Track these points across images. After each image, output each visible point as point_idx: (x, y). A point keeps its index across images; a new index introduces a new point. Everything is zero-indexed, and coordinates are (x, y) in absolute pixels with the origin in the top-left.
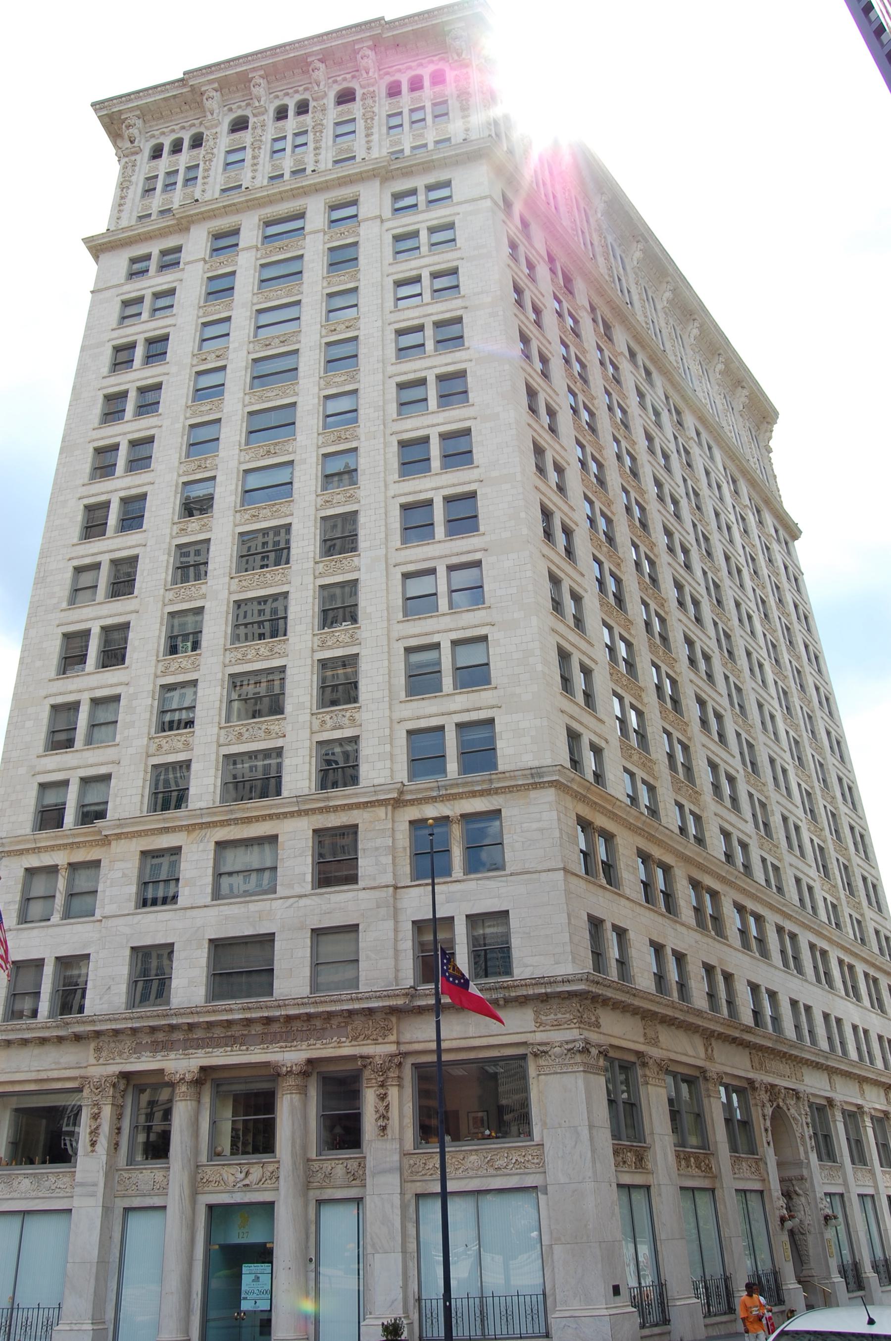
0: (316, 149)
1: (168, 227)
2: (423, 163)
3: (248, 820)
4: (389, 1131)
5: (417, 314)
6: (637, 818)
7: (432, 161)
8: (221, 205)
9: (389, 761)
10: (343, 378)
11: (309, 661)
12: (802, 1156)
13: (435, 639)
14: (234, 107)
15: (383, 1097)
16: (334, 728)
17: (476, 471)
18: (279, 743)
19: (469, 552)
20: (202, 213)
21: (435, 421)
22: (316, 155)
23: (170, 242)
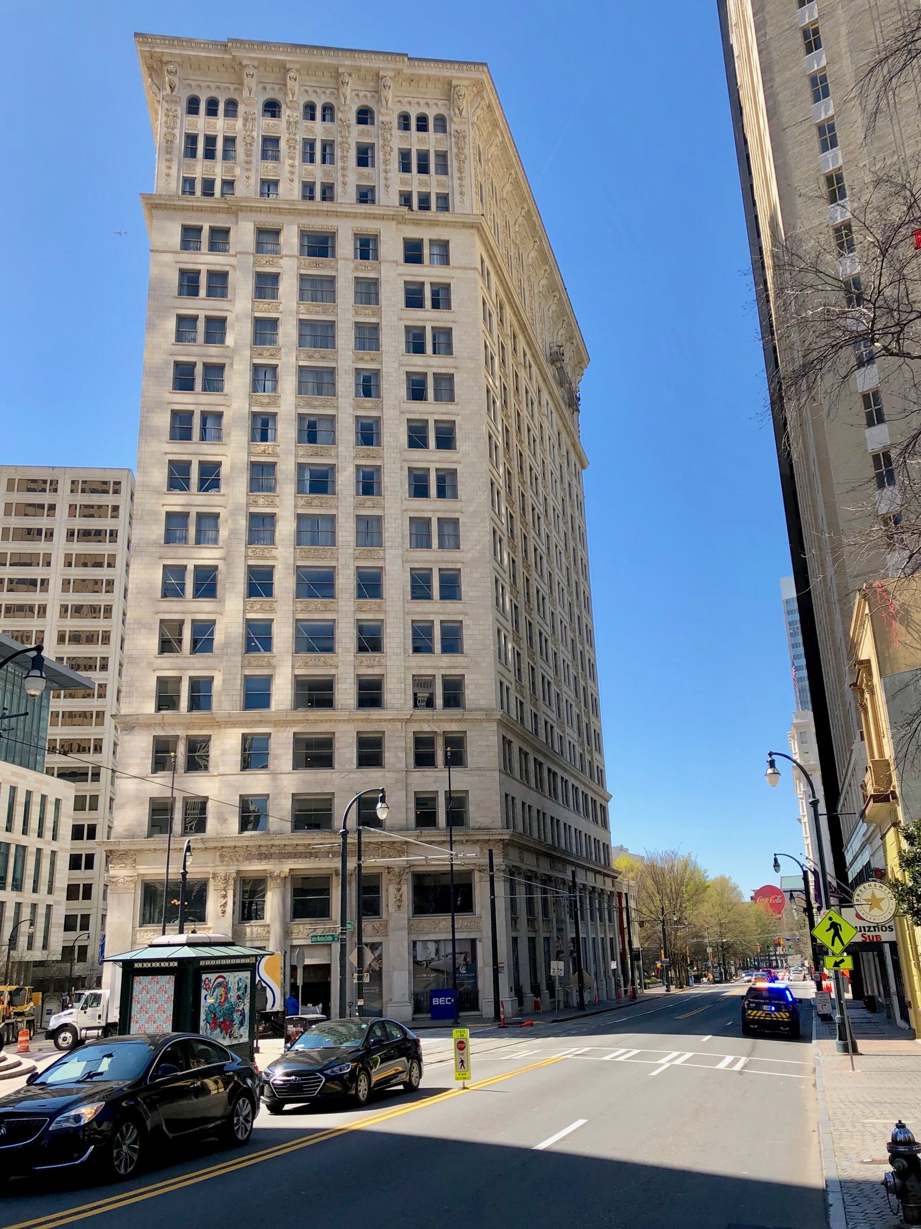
0: (343, 169)
1: (219, 208)
2: (431, 220)
3: (315, 722)
4: (401, 908)
5: (421, 363)
6: (522, 731)
7: (438, 221)
8: (269, 206)
9: (403, 694)
10: (370, 405)
11: (352, 621)
12: (563, 917)
13: (431, 617)
14: (268, 87)
15: (399, 890)
16: (368, 667)
17: (460, 504)
18: (333, 672)
19: (452, 562)
20: (251, 207)
21: (434, 458)
22: (343, 176)
23: (221, 222)
